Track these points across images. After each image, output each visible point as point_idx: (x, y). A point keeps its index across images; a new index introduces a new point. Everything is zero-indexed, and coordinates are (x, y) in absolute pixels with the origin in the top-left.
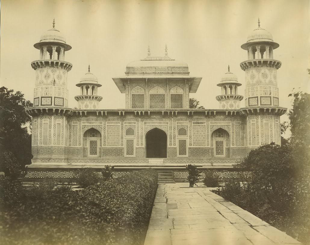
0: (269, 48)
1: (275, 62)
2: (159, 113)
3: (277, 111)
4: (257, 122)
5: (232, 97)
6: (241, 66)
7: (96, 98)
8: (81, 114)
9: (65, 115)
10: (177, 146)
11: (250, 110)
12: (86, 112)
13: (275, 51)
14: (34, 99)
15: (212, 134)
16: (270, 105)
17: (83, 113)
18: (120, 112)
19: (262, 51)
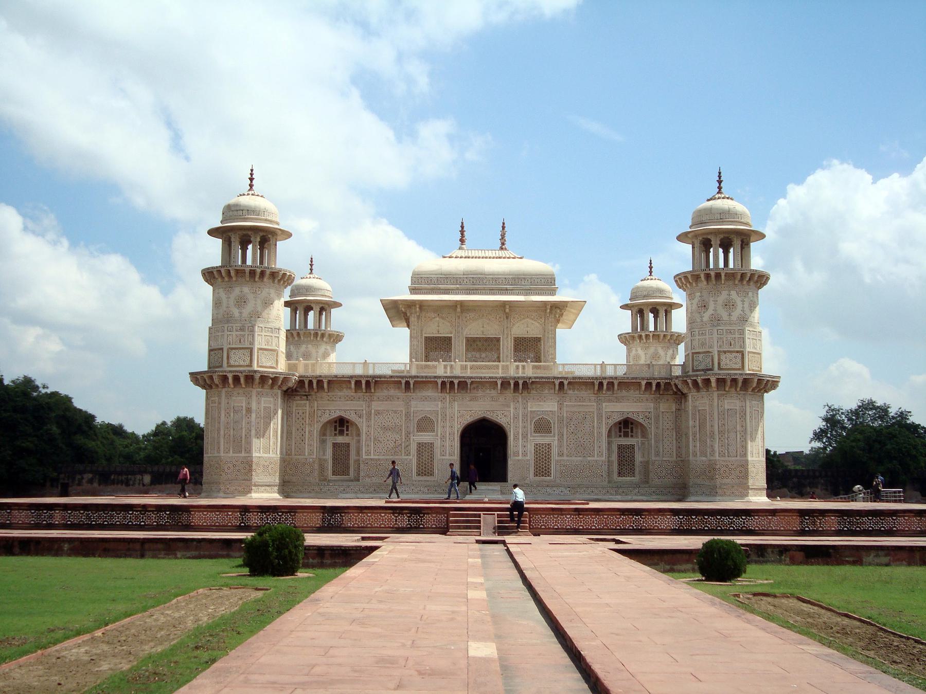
0: (739, 243)
1: (752, 275)
2: (492, 383)
3: (755, 385)
4: (711, 406)
5: (656, 336)
6: (676, 281)
7: (330, 336)
8: (315, 385)
9: (280, 387)
10: (531, 457)
11: (695, 383)
12: (325, 382)
13: (755, 247)
14: (210, 351)
15: (610, 431)
16: (739, 369)
17: (320, 382)
18: (403, 381)
19: (726, 246)
